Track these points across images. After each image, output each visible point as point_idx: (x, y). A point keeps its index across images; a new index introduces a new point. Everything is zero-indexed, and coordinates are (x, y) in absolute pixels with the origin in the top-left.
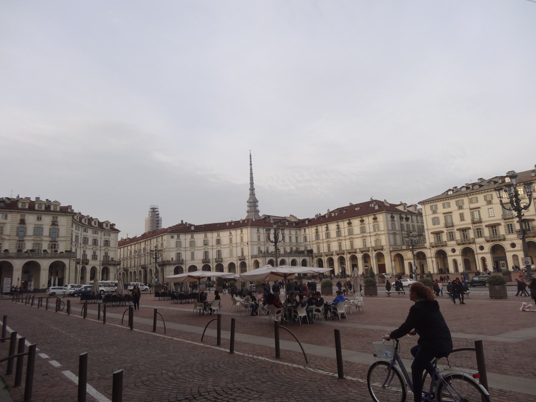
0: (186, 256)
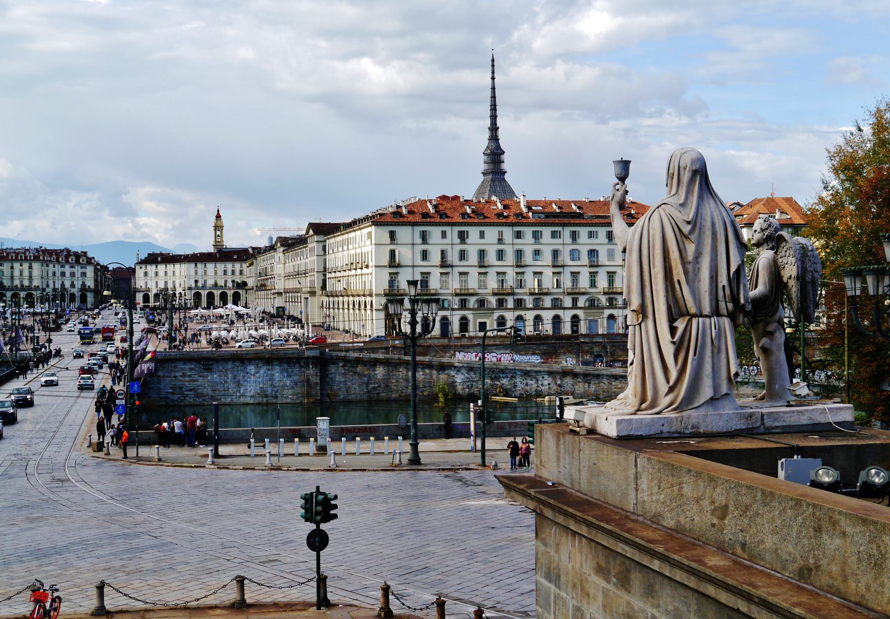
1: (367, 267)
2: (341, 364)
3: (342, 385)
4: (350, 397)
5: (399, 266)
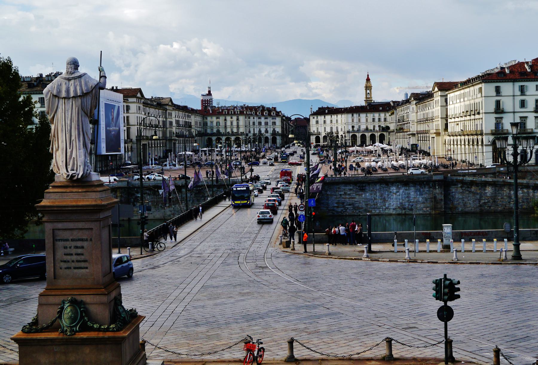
0: (322, 130)
1: (479, 113)
2: (459, 186)
3: (460, 201)
4: (467, 210)
5: (503, 112)
